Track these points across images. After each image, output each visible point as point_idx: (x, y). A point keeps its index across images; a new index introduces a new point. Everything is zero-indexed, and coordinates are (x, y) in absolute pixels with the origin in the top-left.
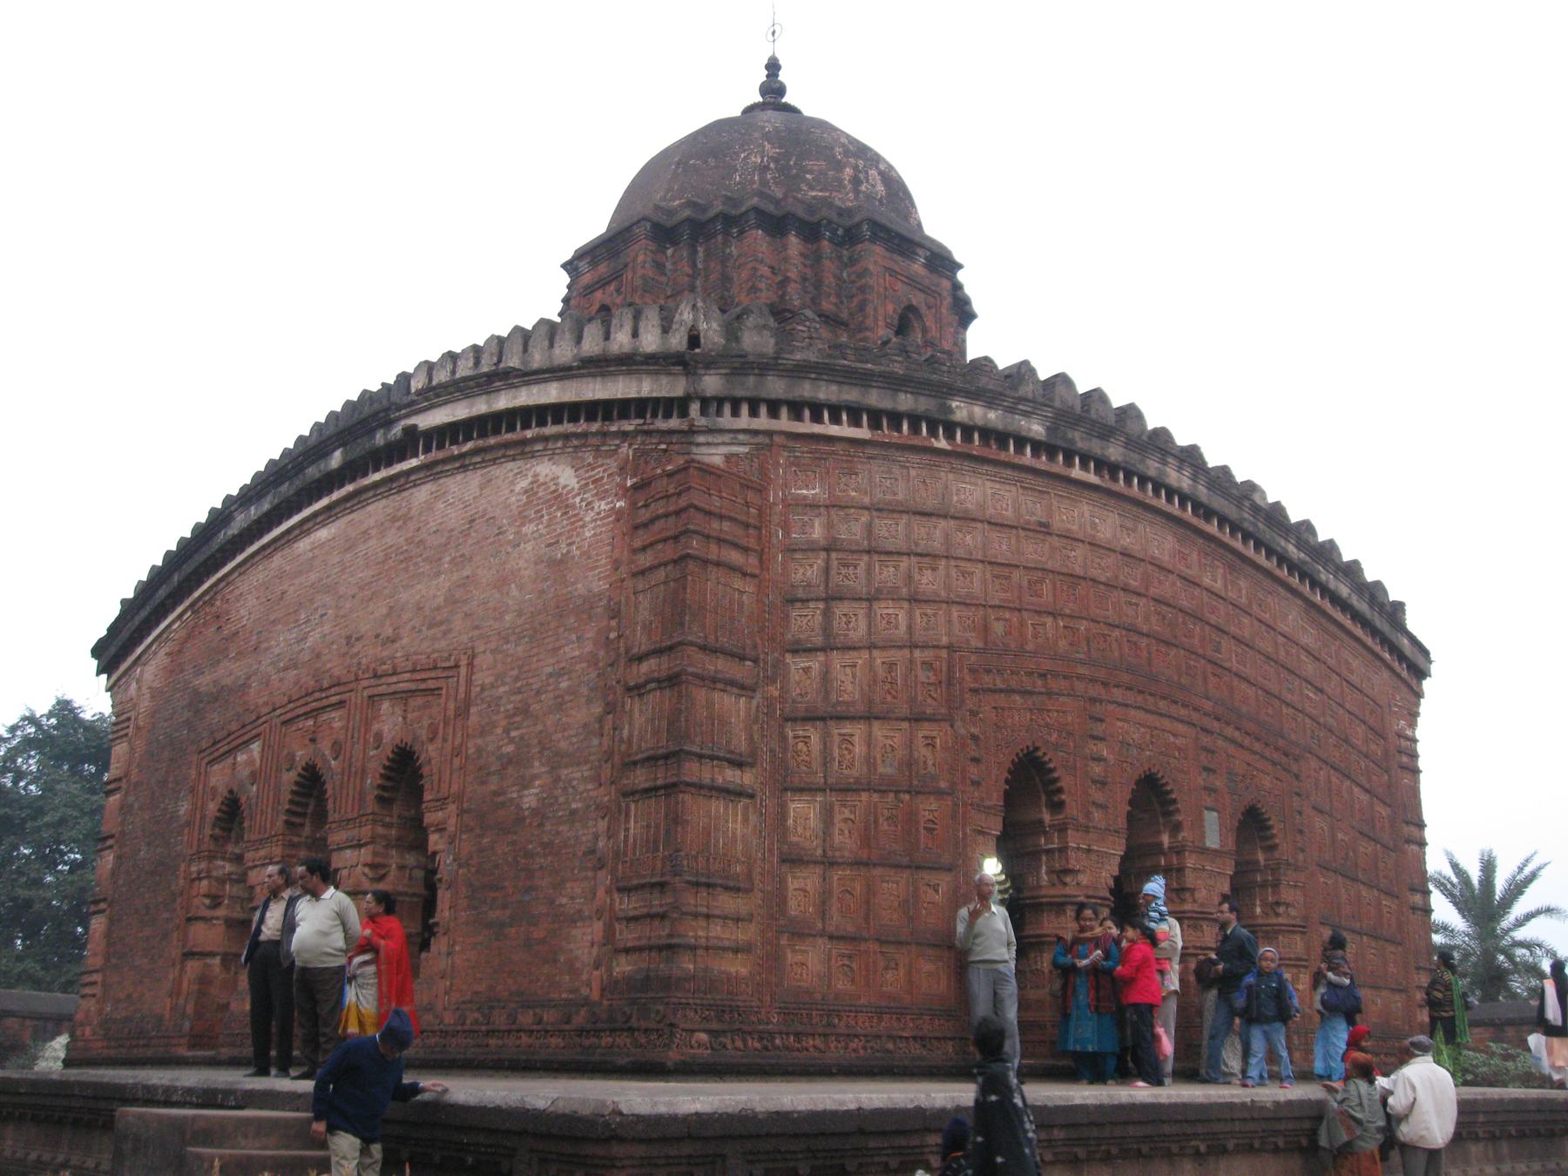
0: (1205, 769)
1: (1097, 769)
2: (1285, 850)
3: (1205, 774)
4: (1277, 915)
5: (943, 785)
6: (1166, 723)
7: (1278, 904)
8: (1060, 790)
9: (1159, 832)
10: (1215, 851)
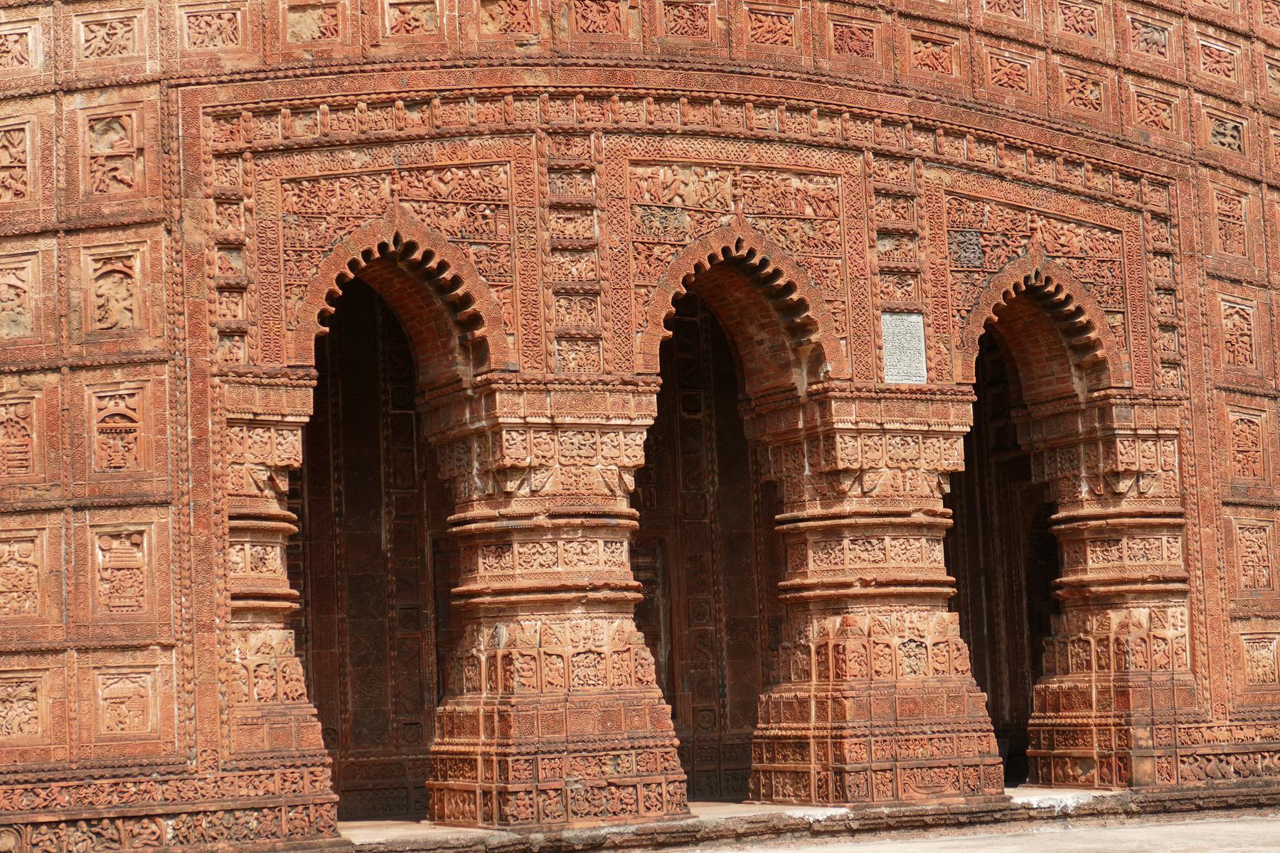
0: (884, 233)
1: (580, 268)
2: (1123, 368)
3: (887, 245)
4: (1120, 496)
5: (148, 345)
6: (780, 155)
7: (1117, 475)
8: (476, 320)
9: (786, 367)
10: (918, 395)
